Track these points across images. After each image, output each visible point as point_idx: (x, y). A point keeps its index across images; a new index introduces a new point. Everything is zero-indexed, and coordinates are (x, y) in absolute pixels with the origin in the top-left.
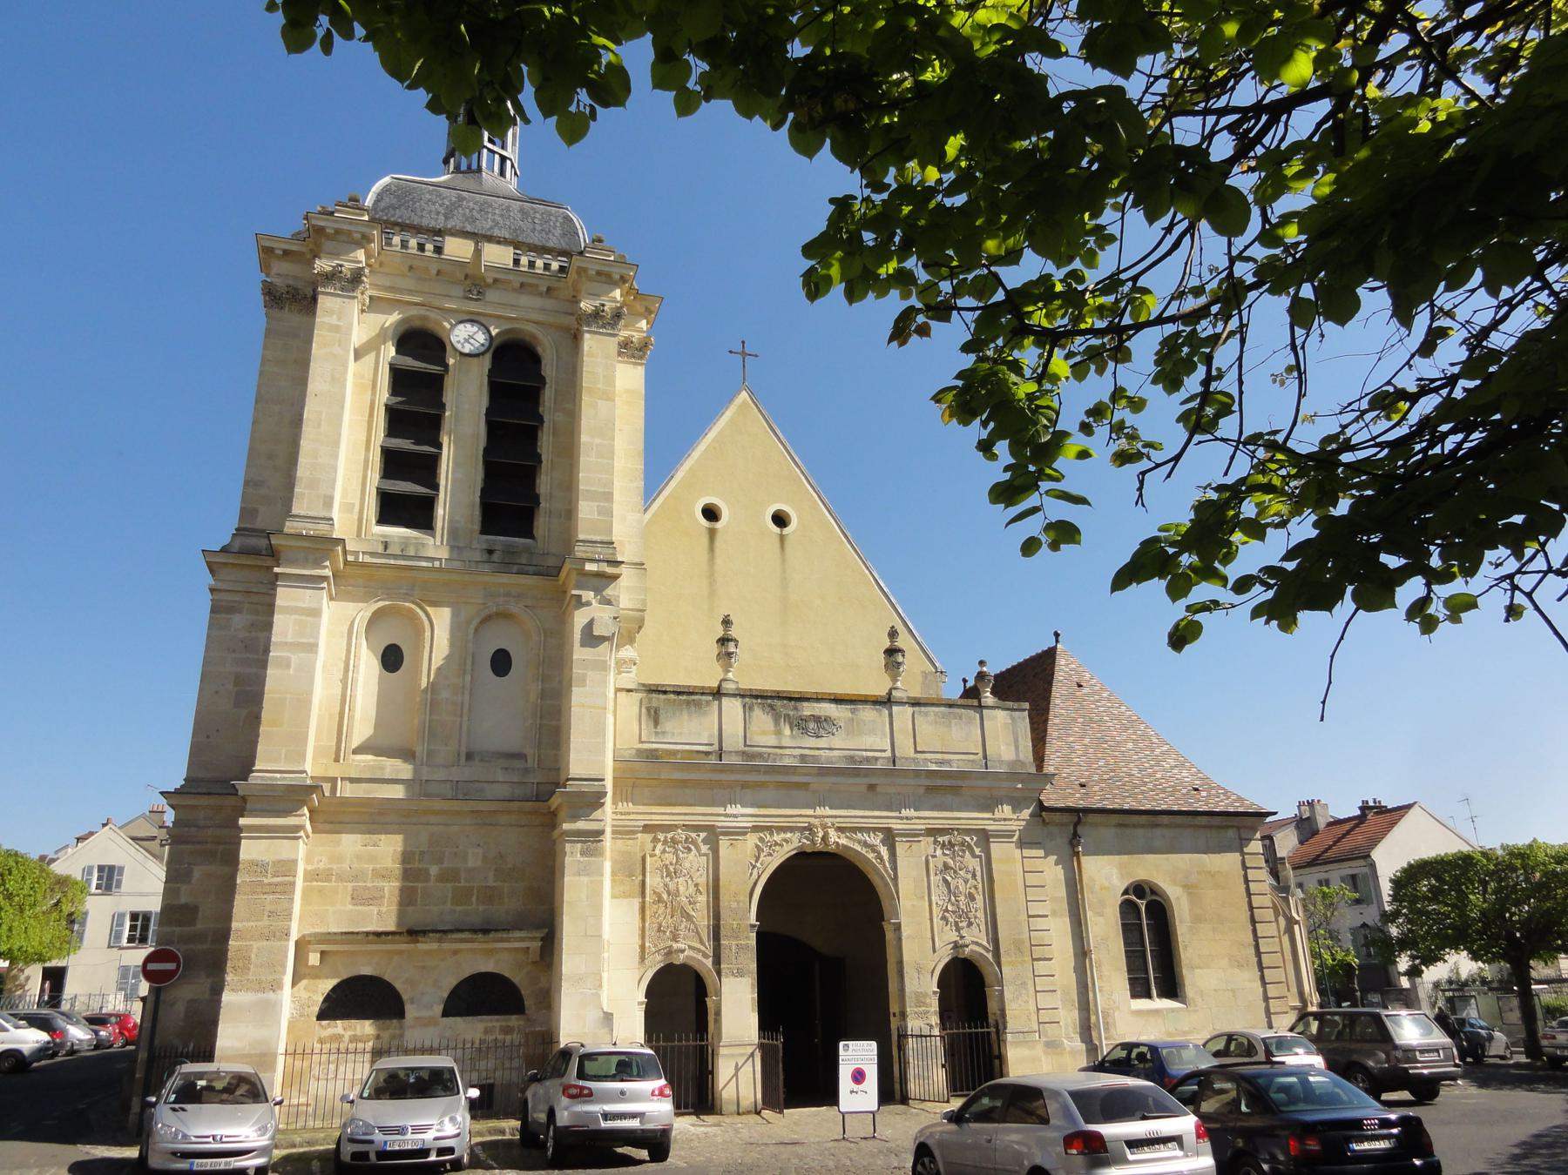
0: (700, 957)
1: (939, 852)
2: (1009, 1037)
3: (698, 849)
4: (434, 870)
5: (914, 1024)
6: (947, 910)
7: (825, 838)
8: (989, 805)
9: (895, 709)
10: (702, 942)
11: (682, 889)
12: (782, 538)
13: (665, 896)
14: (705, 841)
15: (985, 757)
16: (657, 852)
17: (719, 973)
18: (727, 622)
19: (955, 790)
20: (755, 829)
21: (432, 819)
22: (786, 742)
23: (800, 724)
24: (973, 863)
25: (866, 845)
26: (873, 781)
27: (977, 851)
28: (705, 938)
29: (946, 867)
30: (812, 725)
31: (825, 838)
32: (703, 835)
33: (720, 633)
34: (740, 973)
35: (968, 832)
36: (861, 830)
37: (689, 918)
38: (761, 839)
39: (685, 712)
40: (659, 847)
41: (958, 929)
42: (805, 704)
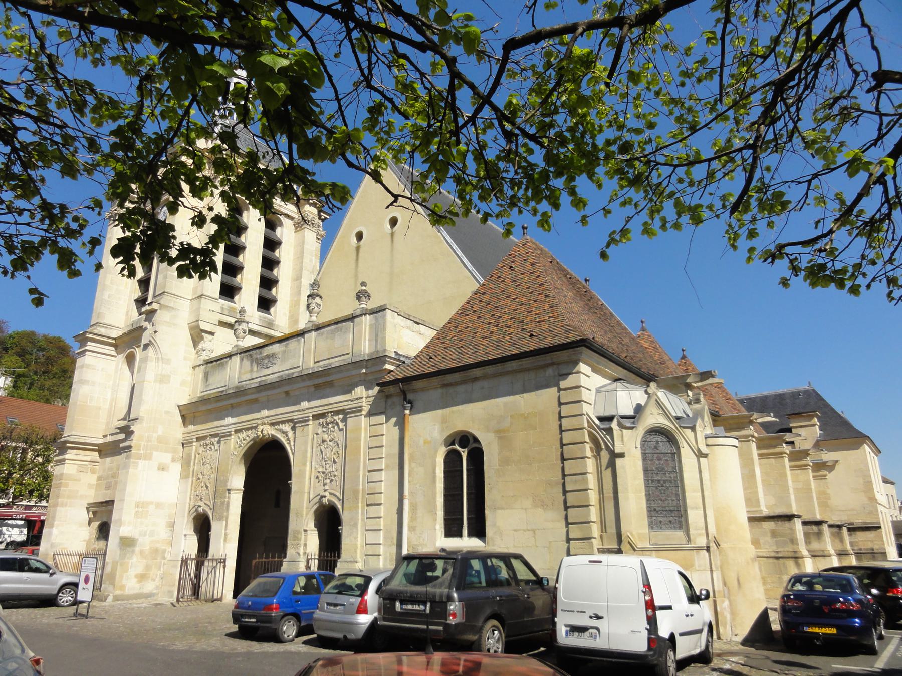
2: (339, 564)
19: (330, 384)
20: (237, 431)
23: (259, 362)
26: (286, 388)
29: (323, 441)
35: (337, 413)
37: (207, 487)
42: (266, 348)
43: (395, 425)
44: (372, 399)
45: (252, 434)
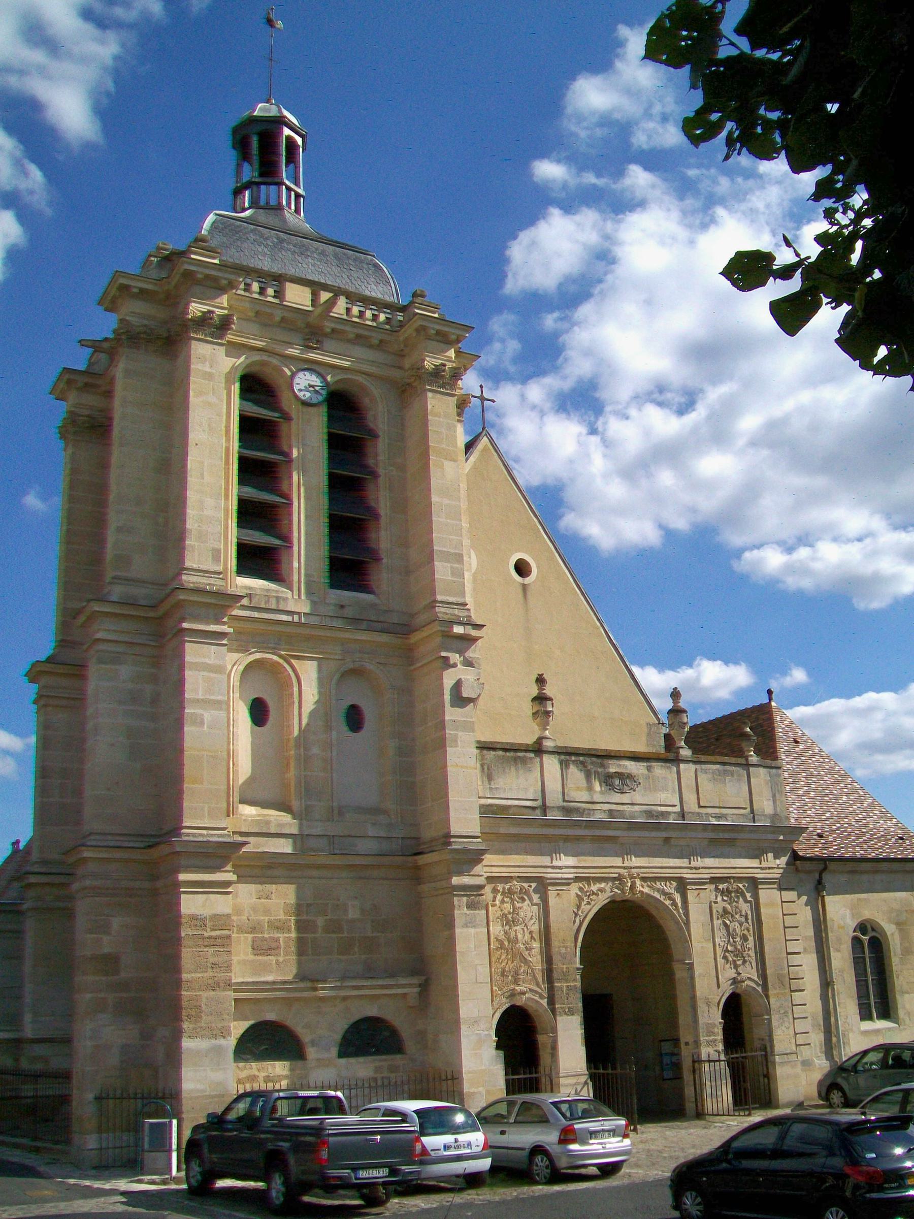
0: (537, 998)
1: (719, 899)
3: (531, 899)
4: (320, 921)
5: (705, 1052)
6: (727, 951)
7: (633, 887)
8: (757, 854)
9: (682, 766)
10: (538, 985)
11: (520, 936)
12: (524, 587)
13: (506, 943)
14: (535, 891)
15: (752, 811)
16: (497, 902)
17: (554, 1011)
18: (541, 681)
19: (731, 842)
21: (315, 873)
22: (597, 798)
23: (608, 780)
24: (745, 907)
27: (748, 895)
28: (540, 979)
30: (617, 782)
32: (534, 885)
33: (535, 691)
34: (571, 1012)
35: (740, 879)
37: (526, 961)
38: (581, 889)
39: (513, 769)
40: (499, 897)
41: (736, 967)
43: (806, 905)
44: (781, 871)
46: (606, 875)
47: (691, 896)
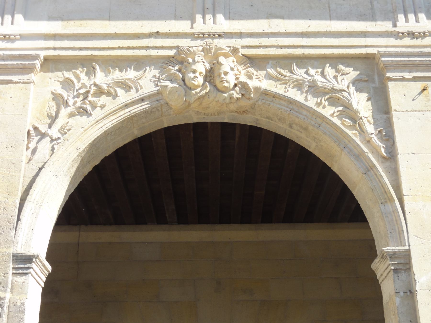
20: (51, 64)
25: (314, 89)
31: (211, 76)
36: (303, 61)
45: (147, 82)
46: (143, 53)
47: (400, 93)
